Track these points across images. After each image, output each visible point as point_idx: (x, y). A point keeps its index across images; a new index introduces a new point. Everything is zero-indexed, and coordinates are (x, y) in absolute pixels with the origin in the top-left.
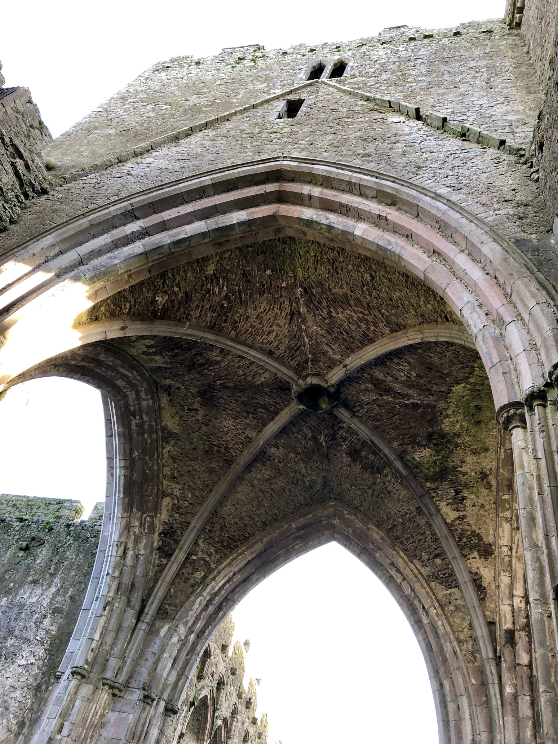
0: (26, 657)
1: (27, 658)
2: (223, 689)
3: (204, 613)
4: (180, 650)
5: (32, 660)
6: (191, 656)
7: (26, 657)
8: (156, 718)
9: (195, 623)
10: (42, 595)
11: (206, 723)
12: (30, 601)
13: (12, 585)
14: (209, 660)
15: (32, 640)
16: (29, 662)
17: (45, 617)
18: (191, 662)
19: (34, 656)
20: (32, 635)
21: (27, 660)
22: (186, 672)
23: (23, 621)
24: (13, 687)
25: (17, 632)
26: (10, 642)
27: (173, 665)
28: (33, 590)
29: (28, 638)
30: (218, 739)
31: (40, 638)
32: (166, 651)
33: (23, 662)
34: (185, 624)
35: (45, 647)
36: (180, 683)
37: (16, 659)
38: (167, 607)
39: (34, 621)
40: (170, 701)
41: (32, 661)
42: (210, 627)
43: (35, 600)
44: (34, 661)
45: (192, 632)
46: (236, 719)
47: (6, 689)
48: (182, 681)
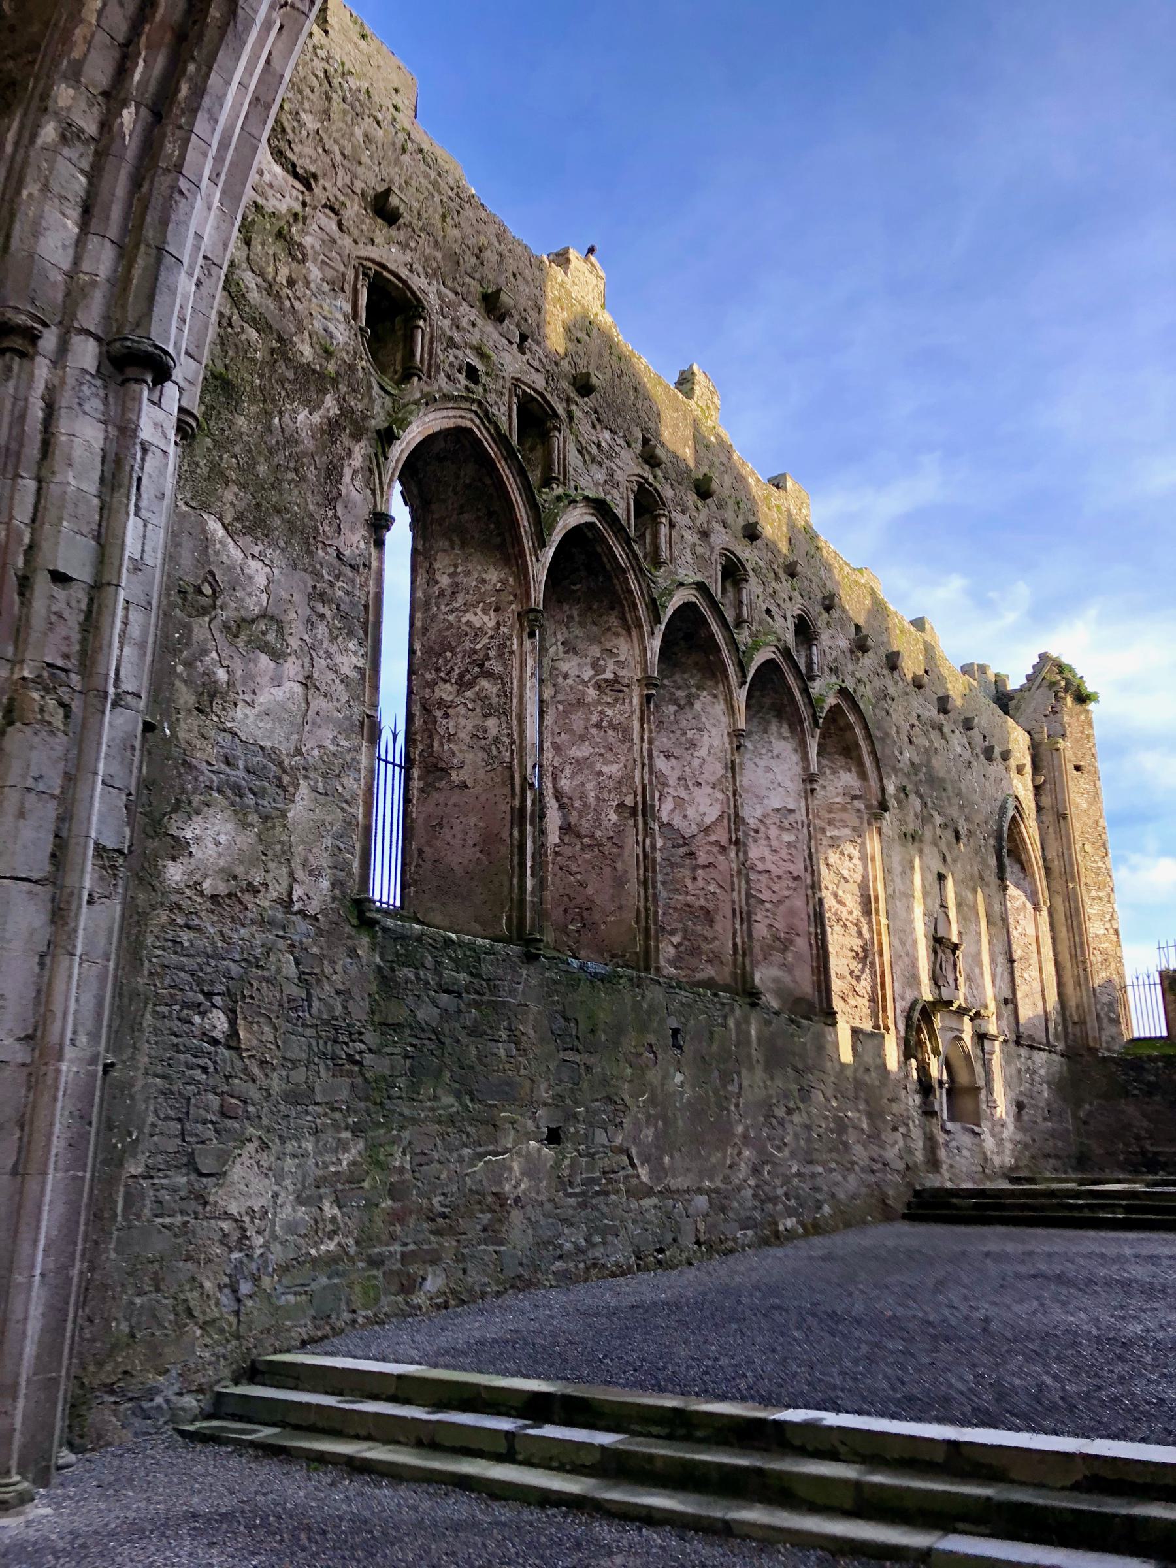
2: (555, 428)
3: (147, 28)
4: (94, 174)
6: (152, 182)
8: (68, 387)
9: (122, 71)
11: (510, 507)
14: (422, 323)
18: (156, 202)
22: (149, 234)
27: (84, 225)
30: (608, 566)
32: (28, 179)
34: (75, 76)
36: (136, 273)
38: (11, 64)
40: (118, 332)
42: (191, 68)
45: (124, 104)
46: (663, 520)
48: (140, 262)
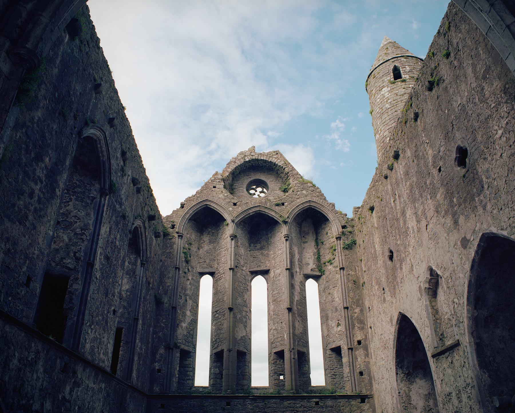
0: (499, 126)
1: (500, 126)
5: (504, 122)
7: (499, 126)
10: (467, 84)
12: (465, 99)
13: (446, 111)
15: (490, 113)
16: (504, 126)
17: (483, 89)
19: (503, 118)
20: (487, 111)
21: (502, 127)
23: (473, 114)
24: (511, 155)
25: (476, 125)
26: (479, 139)
28: (459, 92)
29: (487, 116)
31: (494, 103)
33: (500, 132)
35: (504, 101)
37: (493, 138)
39: (479, 103)
41: (505, 122)
43: (466, 94)
44: (506, 121)
47: (508, 164)
